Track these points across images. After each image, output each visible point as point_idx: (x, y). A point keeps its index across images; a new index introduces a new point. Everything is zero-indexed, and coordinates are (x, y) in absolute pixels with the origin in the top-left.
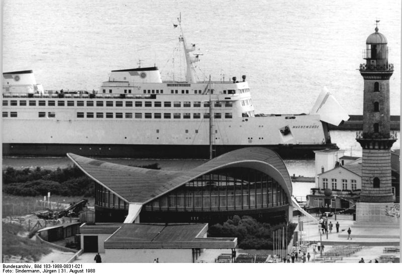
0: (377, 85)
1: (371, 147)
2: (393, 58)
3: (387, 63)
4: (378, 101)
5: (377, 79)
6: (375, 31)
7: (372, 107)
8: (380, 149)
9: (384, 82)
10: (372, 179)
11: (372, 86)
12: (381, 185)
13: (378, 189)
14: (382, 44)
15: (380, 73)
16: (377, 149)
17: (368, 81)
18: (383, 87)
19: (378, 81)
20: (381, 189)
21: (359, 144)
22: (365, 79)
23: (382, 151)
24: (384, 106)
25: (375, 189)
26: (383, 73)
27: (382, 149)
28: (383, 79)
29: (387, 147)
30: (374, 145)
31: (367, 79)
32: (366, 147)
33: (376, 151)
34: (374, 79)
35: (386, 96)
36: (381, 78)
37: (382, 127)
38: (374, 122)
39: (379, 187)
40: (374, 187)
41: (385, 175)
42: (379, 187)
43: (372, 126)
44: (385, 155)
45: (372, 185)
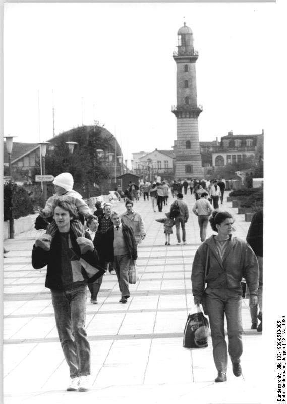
0: (186, 67)
1: (183, 116)
2: (197, 45)
3: (193, 50)
4: (187, 79)
5: (186, 62)
6: (183, 25)
7: (183, 85)
8: (190, 117)
9: (192, 64)
10: (185, 142)
17: (179, 64)
19: (186, 63)
20: (192, 150)
21: (173, 115)
22: (177, 63)
28: (191, 62)
30: (186, 114)
31: (179, 63)
34: (184, 62)
39: (190, 148)
42: (190, 148)
43: (184, 99)
45: (185, 147)
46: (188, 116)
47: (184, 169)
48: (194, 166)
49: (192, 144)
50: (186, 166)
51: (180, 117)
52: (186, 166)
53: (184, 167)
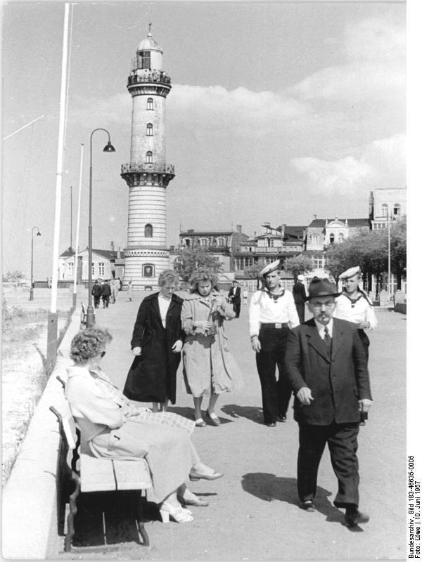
21: (124, 182)
39: (152, 236)
40: (146, 236)
47: (141, 271)
49: (154, 230)
51: (135, 183)
53: (141, 267)
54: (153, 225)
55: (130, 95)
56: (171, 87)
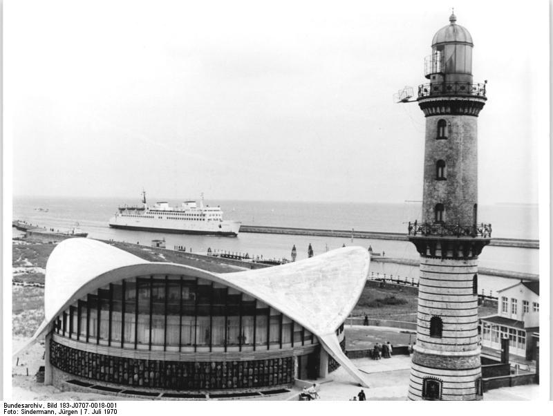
2: (482, 69)
3: (469, 84)
4: (443, 158)
8: (444, 257)
9: (459, 120)
10: (429, 318)
11: (434, 127)
12: (444, 334)
13: (438, 341)
14: (456, 43)
15: (447, 99)
16: (437, 257)
18: (454, 130)
20: (445, 341)
23: (449, 262)
24: (456, 170)
25: (434, 340)
26: (453, 99)
27: (450, 258)
28: (455, 112)
29: (470, 255)
32: (428, 253)
33: (438, 261)
35: (461, 148)
36: (449, 110)
37: (451, 211)
38: (434, 201)
41: (455, 313)
42: (440, 336)
43: (432, 210)
44: (457, 270)
45: (428, 332)
46: (438, 253)
48: (445, 385)
49: (446, 327)
50: (425, 380)
52: (425, 380)
53: (421, 381)
54: (444, 320)
55: (422, 113)
56: (486, 99)
